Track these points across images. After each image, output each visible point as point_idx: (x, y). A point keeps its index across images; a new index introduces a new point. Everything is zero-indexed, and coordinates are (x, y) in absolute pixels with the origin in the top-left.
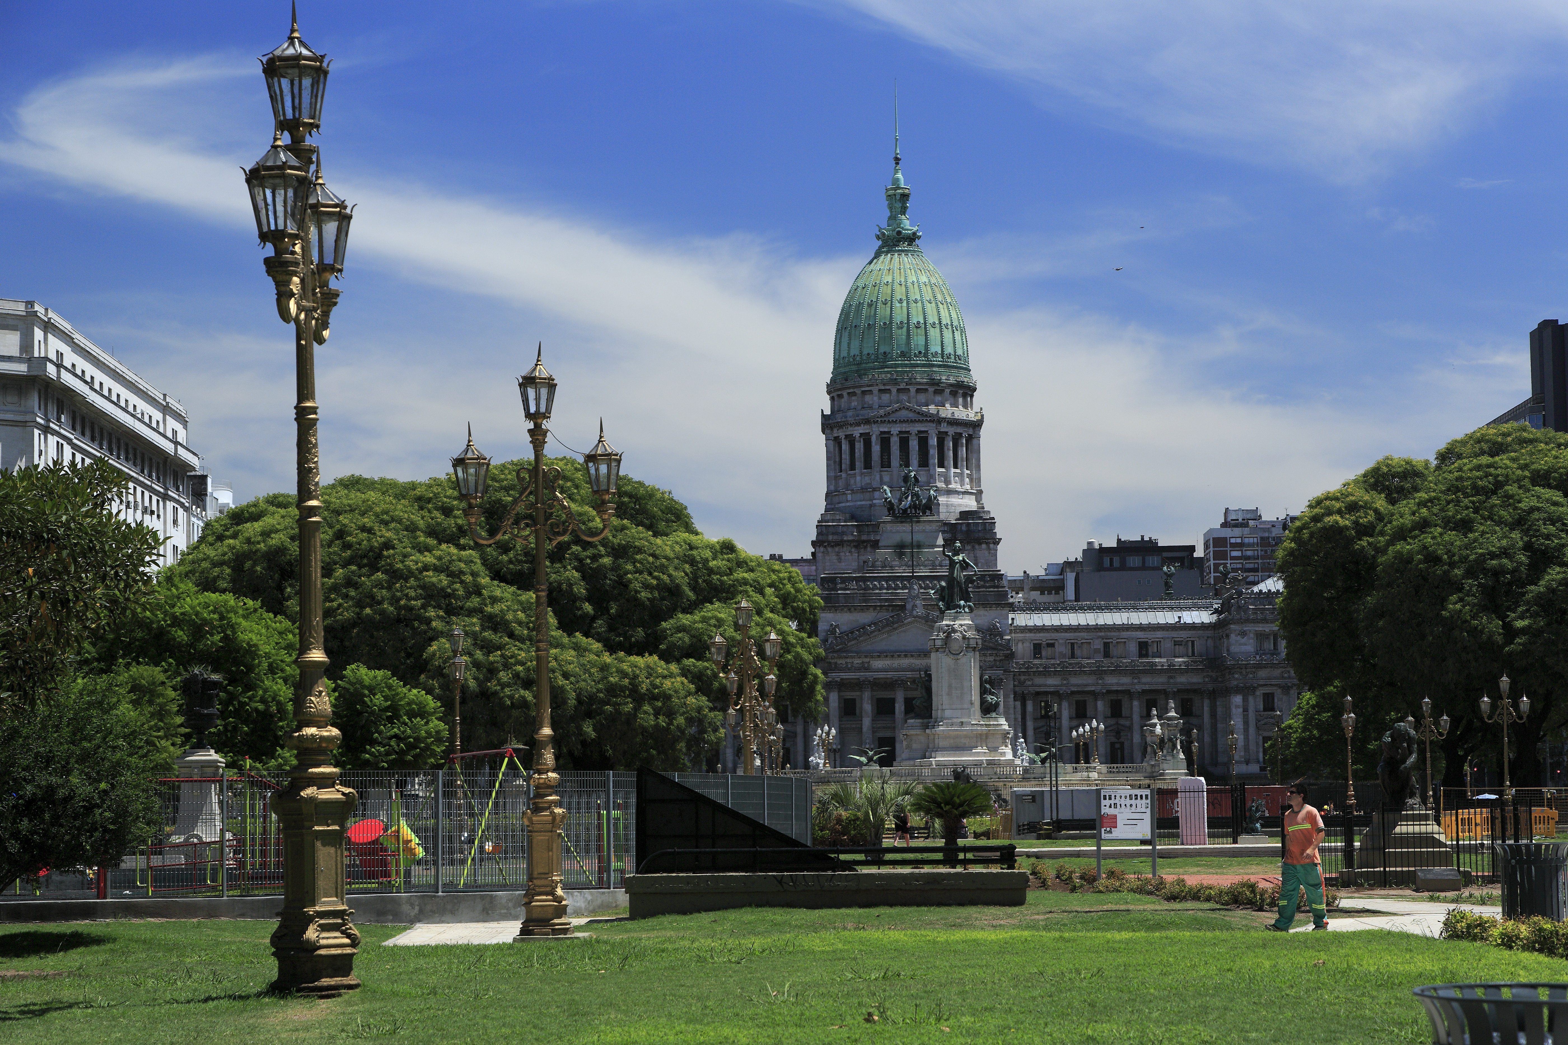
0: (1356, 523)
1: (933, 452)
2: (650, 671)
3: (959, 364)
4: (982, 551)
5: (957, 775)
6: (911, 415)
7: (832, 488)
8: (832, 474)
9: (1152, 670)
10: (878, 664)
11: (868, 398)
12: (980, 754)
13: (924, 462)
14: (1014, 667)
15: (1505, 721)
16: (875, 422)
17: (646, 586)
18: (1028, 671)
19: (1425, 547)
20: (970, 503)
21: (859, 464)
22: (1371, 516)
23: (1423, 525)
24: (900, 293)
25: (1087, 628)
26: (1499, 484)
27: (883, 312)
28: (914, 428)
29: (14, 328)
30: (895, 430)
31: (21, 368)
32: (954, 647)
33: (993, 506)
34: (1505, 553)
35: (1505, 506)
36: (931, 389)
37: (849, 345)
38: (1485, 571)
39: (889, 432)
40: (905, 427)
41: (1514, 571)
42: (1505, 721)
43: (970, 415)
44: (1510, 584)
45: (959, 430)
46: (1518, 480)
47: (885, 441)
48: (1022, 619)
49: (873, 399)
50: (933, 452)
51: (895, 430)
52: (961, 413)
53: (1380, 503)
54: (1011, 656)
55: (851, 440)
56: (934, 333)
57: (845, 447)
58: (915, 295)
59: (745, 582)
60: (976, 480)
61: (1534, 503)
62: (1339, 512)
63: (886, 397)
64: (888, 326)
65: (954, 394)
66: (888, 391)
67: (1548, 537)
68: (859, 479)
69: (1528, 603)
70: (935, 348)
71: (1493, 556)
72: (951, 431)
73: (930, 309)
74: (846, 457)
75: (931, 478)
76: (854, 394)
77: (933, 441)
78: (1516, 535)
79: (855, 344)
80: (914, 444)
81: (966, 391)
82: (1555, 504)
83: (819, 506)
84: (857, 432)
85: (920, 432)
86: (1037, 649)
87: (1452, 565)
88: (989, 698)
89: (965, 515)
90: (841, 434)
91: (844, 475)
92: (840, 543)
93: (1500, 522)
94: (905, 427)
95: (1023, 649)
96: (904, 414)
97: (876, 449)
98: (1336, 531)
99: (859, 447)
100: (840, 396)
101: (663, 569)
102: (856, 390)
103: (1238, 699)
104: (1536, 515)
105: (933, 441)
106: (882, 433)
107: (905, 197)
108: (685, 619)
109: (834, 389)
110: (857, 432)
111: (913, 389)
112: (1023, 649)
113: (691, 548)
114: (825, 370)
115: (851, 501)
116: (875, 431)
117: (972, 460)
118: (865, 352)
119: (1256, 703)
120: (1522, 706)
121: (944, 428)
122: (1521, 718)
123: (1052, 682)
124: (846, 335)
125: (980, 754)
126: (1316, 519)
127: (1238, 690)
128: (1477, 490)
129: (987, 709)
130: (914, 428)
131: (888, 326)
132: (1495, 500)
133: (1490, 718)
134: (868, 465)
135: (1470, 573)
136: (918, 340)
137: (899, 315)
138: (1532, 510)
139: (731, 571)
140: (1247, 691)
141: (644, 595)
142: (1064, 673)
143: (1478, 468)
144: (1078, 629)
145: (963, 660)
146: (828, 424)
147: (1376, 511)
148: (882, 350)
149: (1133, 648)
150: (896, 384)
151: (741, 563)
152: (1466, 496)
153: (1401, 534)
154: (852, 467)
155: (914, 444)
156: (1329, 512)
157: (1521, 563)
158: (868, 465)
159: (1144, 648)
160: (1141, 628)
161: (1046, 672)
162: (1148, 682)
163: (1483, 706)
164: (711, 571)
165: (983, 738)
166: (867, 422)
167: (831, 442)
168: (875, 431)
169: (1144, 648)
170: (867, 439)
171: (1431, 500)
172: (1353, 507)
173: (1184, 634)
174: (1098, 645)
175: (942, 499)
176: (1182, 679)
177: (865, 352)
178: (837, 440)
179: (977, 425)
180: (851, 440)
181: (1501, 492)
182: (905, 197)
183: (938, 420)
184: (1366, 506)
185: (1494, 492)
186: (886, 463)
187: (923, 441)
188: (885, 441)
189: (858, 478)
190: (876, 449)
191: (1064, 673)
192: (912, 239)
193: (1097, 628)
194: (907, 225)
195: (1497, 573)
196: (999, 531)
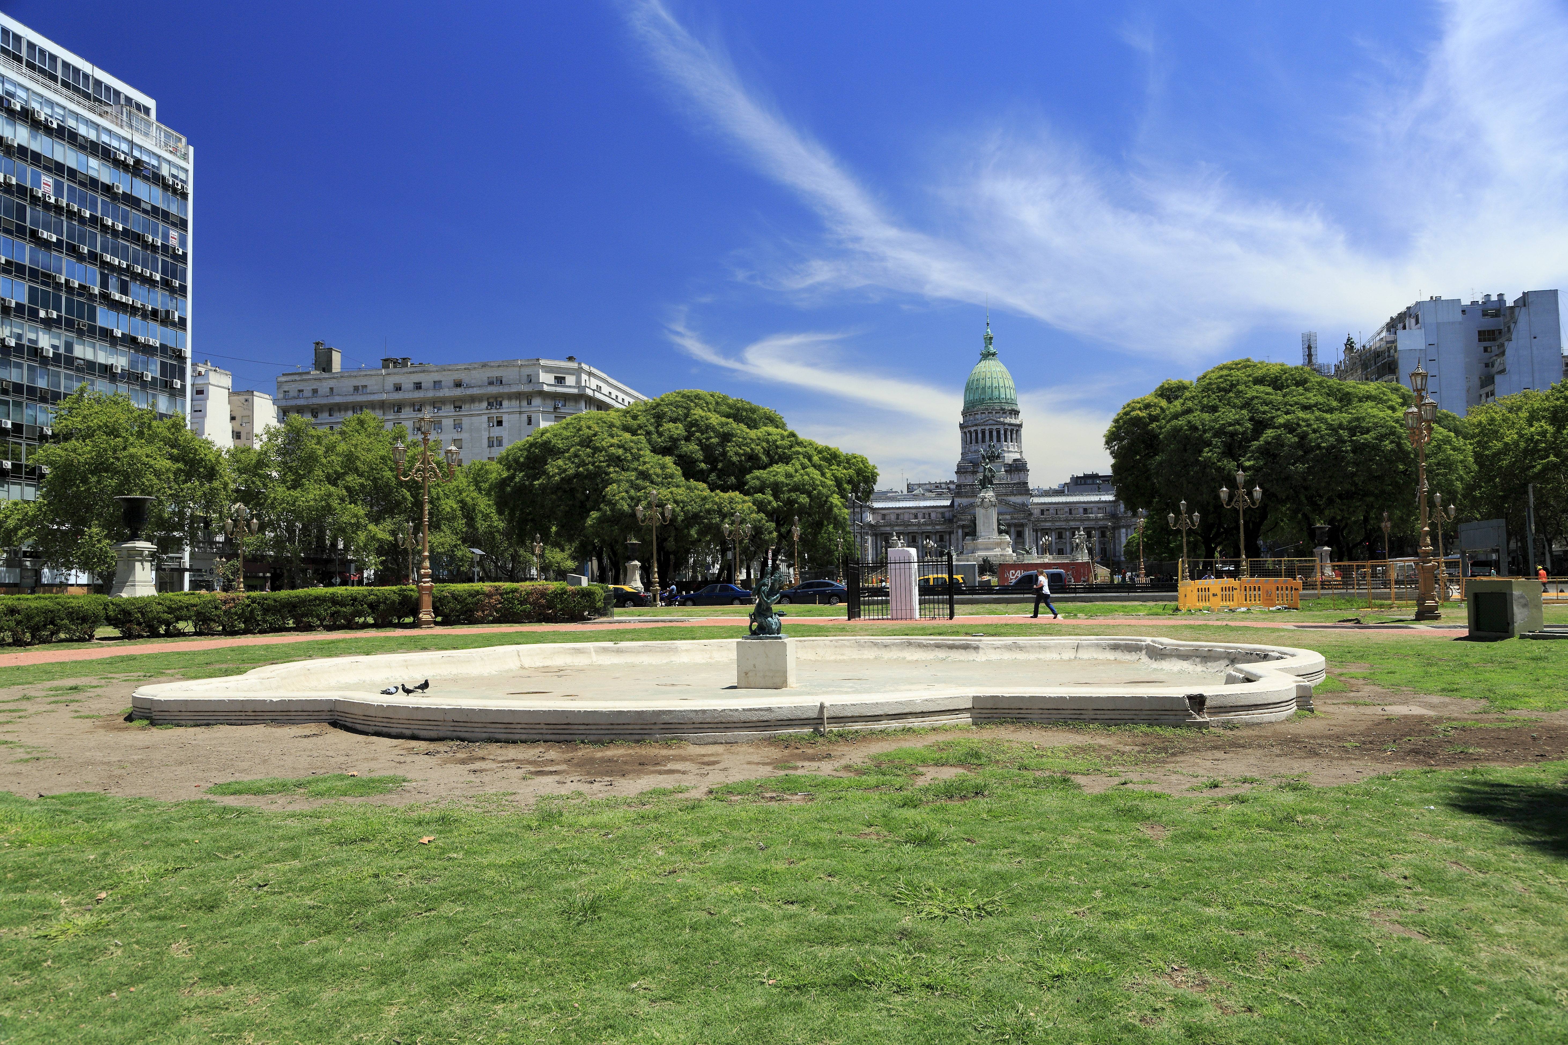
0: (1150, 415)
1: (1002, 437)
2: (731, 501)
3: (1013, 402)
4: (1022, 474)
5: (984, 561)
9: (1089, 519)
12: (997, 551)
13: (999, 440)
14: (1032, 519)
15: (1241, 507)
17: (736, 454)
18: (1038, 520)
19: (1189, 422)
20: (1017, 456)
22: (1158, 411)
23: (1189, 411)
24: (989, 375)
25: (1063, 503)
26: (1233, 386)
27: (982, 382)
28: (995, 427)
29: (573, 374)
30: (987, 428)
31: (575, 391)
32: (986, 505)
33: (1027, 457)
34: (1238, 422)
35: (1237, 397)
38: (1225, 433)
41: (1243, 433)
42: (1241, 507)
43: (1018, 422)
44: (1240, 442)
46: (1245, 383)
47: (983, 432)
48: (1036, 500)
50: (1002, 437)
51: (987, 428)
52: (1013, 421)
53: (1164, 403)
54: (1031, 514)
56: (1002, 390)
58: (994, 375)
59: (798, 453)
60: (1020, 447)
61: (1255, 394)
62: (1140, 409)
64: (984, 388)
67: (1264, 413)
68: (974, 447)
69: (1252, 451)
70: (1003, 396)
71: (1230, 425)
73: (1001, 381)
75: (1002, 446)
77: (1002, 432)
78: (1244, 412)
80: (995, 433)
81: (1016, 413)
82: (1267, 394)
83: (959, 458)
84: (972, 429)
86: (1042, 512)
87: (1205, 431)
88: (1002, 527)
89: (1015, 460)
92: (966, 472)
93: (1234, 407)
95: (1036, 512)
97: (980, 435)
98: (1138, 419)
99: (974, 435)
101: (746, 445)
103: (1123, 530)
104: (1256, 401)
105: (1002, 432)
107: (991, 338)
108: (757, 473)
109: (965, 413)
110: (972, 429)
112: (1036, 512)
113: (769, 434)
115: (970, 456)
116: (979, 428)
117: (1018, 439)
120: (1255, 494)
122: (1253, 503)
123: (1048, 525)
125: (997, 551)
126: (1126, 414)
127: (1123, 527)
128: (1220, 389)
129: (1000, 532)
130: (995, 427)
131: (984, 388)
132: (1231, 394)
133: (1228, 504)
134: (977, 442)
135: (1216, 435)
136: (996, 393)
137: (988, 384)
138: (1253, 398)
139: (791, 447)
141: (735, 459)
142: (1053, 521)
143: (1221, 377)
144: (1058, 503)
145: (990, 510)
146: (962, 426)
147: (1161, 408)
149: (1081, 510)
151: (800, 444)
152: (1214, 393)
153: (1176, 416)
155: (995, 433)
156: (1133, 409)
157: (1247, 428)
158: (977, 442)
159: (1085, 510)
160: (1084, 503)
161: (1045, 521)
162: (1087, 524)
163: (1222, 495)
164: (777, 447)
165: (999, 544)
168: (979, 428)
169: (1085, 510)
171: (1193, 397)
172: (1147, 406)
173: (1101, 505)
174: (1067, 510)
175: (1006, 455)
176: (1101, 523)
179: (1020, 426)
181: (1234, 390)
182: (991, 338)
183: (1004, 424)
184: (1155, 405)
185: (1230, 391)
186: (983, 441)
187: (998, 432)
188: (983, 432)
190: (980, 435)
191: (1053, 521)
192: (994, 354)
193: (1066, 503)
194: (992, 349)
195: (1233, 435)
196: (1028, 467)
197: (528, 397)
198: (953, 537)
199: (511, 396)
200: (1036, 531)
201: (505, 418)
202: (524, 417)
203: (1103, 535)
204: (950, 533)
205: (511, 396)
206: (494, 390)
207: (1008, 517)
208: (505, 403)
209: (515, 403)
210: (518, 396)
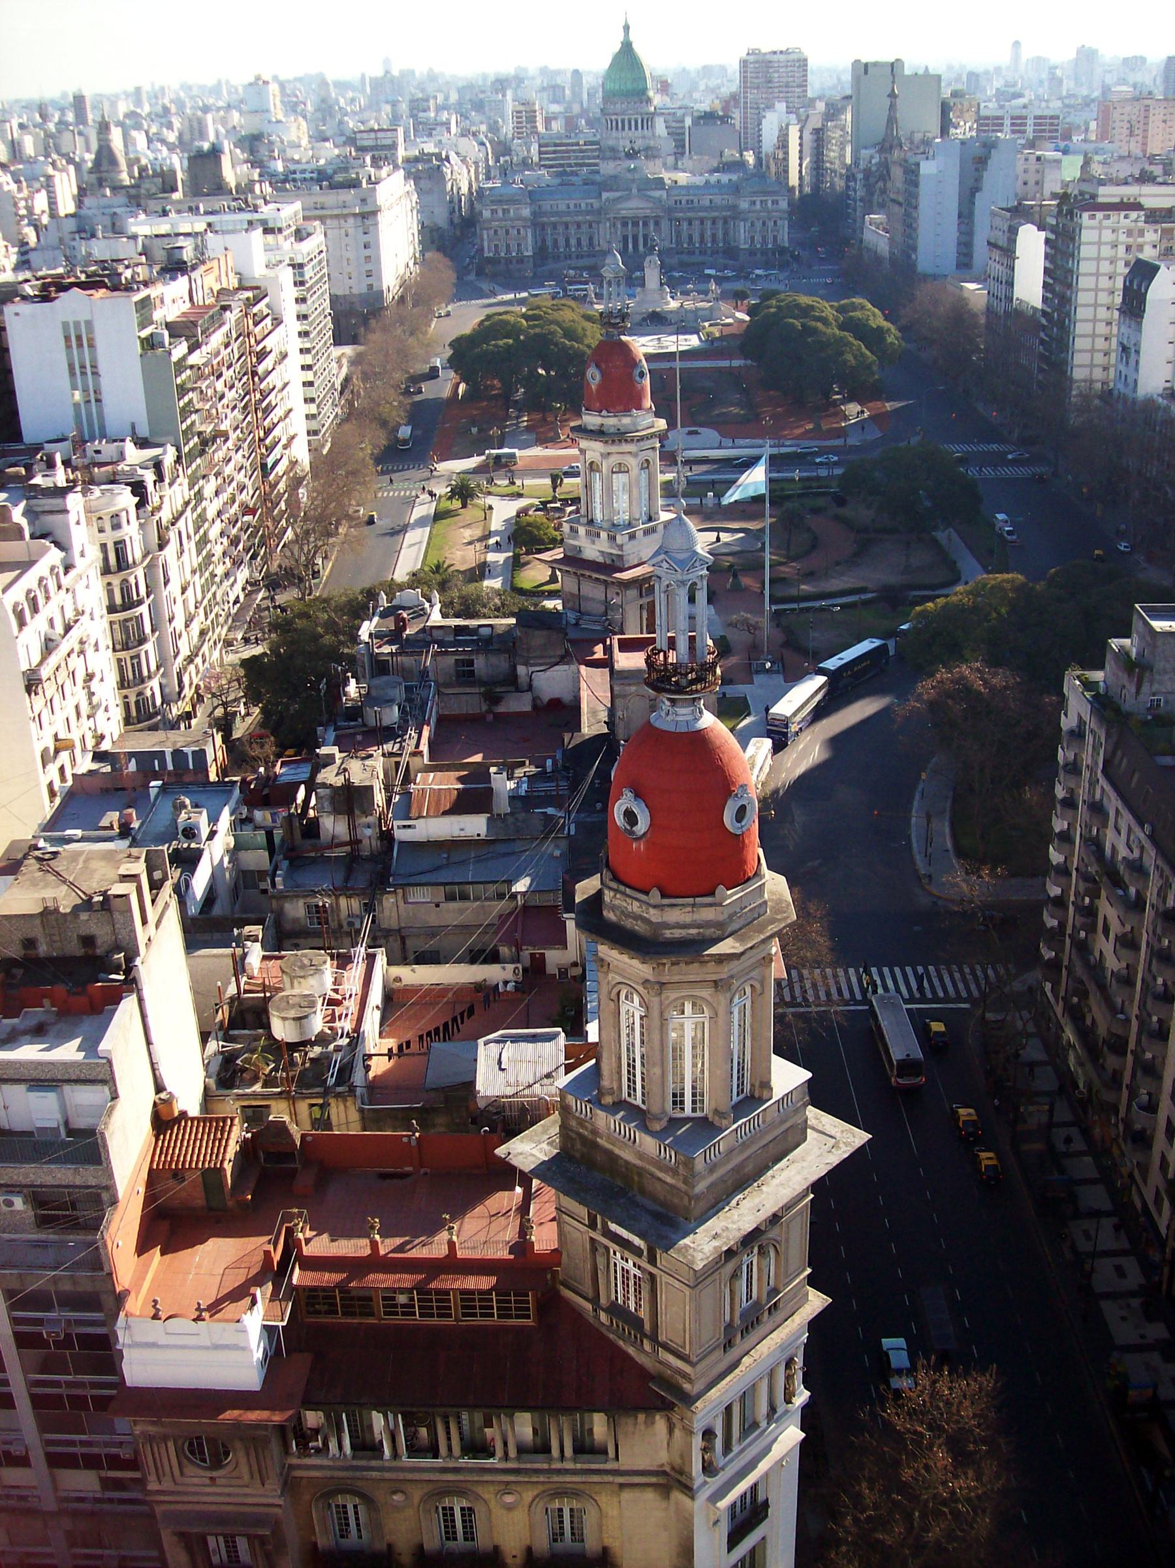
49: (618, 106)
80: (633, 123)
103: (742, 223)
110: (613, 117)
119: (748, 224)
140: (745, 220)
155: (633, 123)
186: (623, 129)
197: (345, 217)
198: (601, 225)
199: (332, 217)
200: (670, 220)
201: (329, 232)
202: (343, 231)
203: (726, 222)
204: (598, 223)
205: (332, 217)
206: (318, 213)
208: (328, 221)
209: (335, 223)
210: (337, 217)
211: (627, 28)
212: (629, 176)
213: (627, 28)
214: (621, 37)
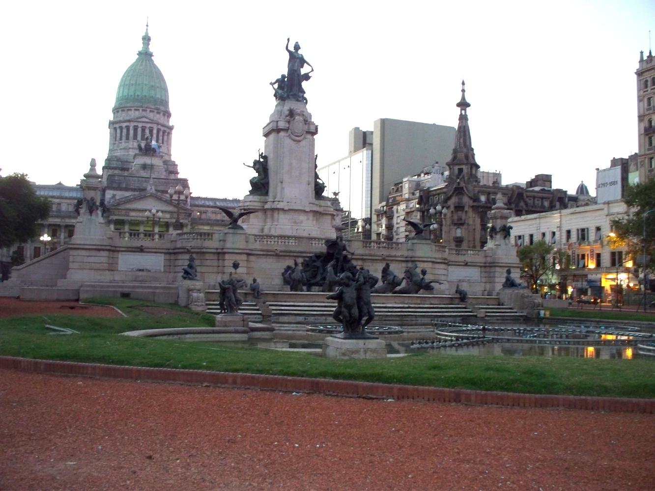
6: (147, 120)
7: (112, 148)
8: (112, 142)
10: (132, 214)
11: (129, 112)
16: (133, 121)
21: (124, 138)
28: (148, 125)
30: (140, 125)
36: (156, 111)
37: (123, 92)
39: (137, 126)
40: (144, 125)
45: (165, 129)
47: (136, 128)
51: (140, 125)
55: (121, 128)
57: (118, 131)
63: (137, 112)
65: (164, 115)
66: (138, 110)
68: (124, 145)
72: (162, 128)
74: (118, 135)
76: (123, 111)
77: (155, 131)
79: (126, 91)
84: (124, 125)
85: (150, 127)
90: (117, 126)
91: (117, 142)
94: (144, 125)
96: (144, 120)
97: (132, 132)
99: (125, 131)
100: (118, 112)
102: (125, 109)
105: (155, 131)
106: (135, 126)
109: (116, 110)
110: (124, 125)
111: (148, 110)
114: (112, 103)
116: (132, 125)
118: (130, 94)
121: (160, 127)
124: (122, 88)
130: (148, 125)
134: (127, 138)
148: (136, 94)
150: (142, 107)
154: (121, 139)
158: (127, 138)
166: (129, 121)
167: (112, 130)
168: (132, 125)
170: (128, 128)
177: (130, 94)
178: (115, 129)
180: (121, 128)
188: (136, 128)
189: (123, 144)
190: (132, 132)
207: (168, 216)
211: (147, 39)
212: (143, 174)
213: (147, 39)
214: (140, 47)
